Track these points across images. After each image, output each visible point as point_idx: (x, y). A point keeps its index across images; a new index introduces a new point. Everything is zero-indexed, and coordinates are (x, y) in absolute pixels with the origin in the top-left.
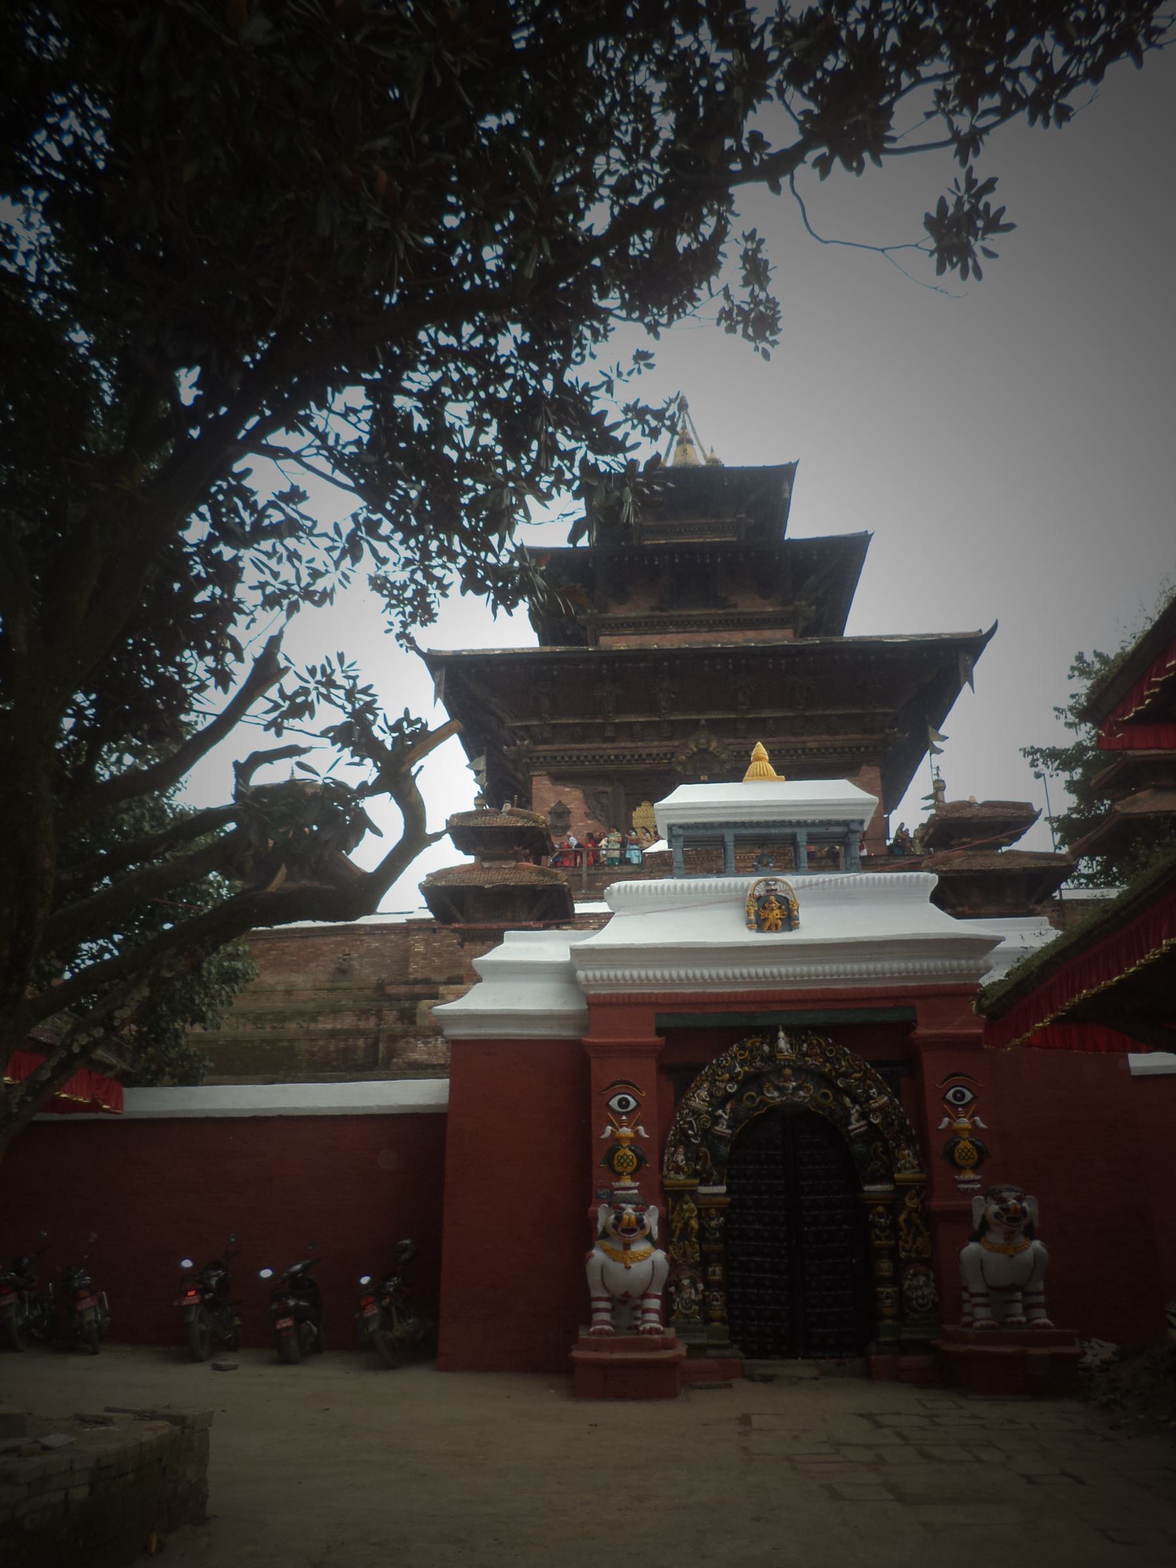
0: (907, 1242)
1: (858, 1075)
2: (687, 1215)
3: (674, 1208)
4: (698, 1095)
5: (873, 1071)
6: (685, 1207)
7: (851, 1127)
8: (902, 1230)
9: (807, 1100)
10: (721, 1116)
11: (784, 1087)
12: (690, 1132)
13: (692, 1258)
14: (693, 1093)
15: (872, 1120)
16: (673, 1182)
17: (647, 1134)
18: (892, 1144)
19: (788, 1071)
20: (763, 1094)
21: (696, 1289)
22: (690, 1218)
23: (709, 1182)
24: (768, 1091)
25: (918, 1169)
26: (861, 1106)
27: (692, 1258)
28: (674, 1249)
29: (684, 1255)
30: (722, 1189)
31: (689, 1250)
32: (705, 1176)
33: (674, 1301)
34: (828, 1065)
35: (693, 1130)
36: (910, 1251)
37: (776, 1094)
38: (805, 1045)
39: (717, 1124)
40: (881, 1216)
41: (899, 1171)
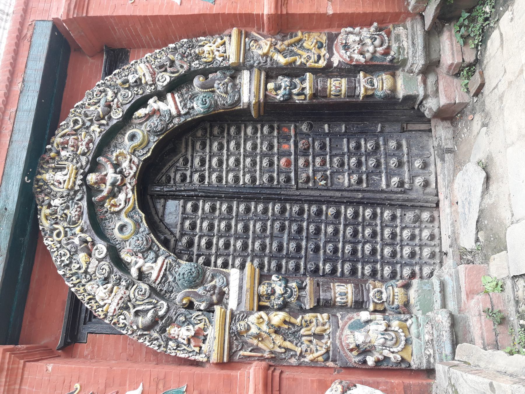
0: (309, 58)
1: (110, 93)
2: (264, 327)
3: (256, 349)
4: (103, 300)
5: (108, 78)
6: (254, 330)
7: (174, 112)
8: (294, 62)
9: (136, 160)
10: (139, 269)
11: (113, 184)
12: (150, 314)
13: (323, 325)
14: (99, 307)
15: (165, 83)
16: (215, 348)
17: (137, 388)
18: (195, 64)
19: (92, 178)
20: (118, 213)
21: (368, 322)
22: (269, 324)
23: (224, 293)
24: (115, 205)
25: (226, 39)
26: (150, 96)
27: (323, 325)
28: (312, 352)
29: (319, 336)
30: (234, 274)
31: (315, 329)
32: (214, 298)
33: (386, 358)
34: (92, 128)
35: (148, 310)
36: (319, 57)
37: (122, 197)
38: (63, 153)
39: (148, 276)
40: (278, 88)
41: (225, 59)
